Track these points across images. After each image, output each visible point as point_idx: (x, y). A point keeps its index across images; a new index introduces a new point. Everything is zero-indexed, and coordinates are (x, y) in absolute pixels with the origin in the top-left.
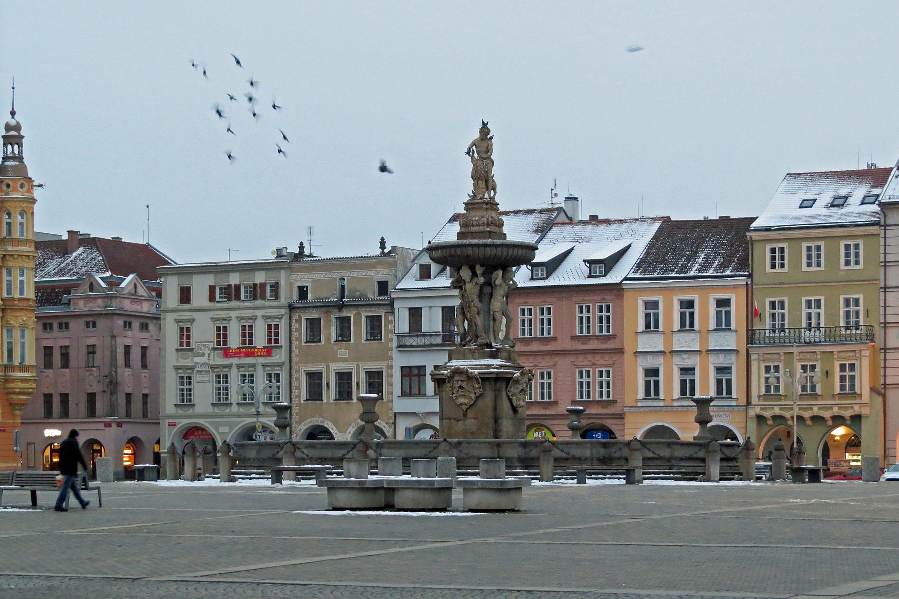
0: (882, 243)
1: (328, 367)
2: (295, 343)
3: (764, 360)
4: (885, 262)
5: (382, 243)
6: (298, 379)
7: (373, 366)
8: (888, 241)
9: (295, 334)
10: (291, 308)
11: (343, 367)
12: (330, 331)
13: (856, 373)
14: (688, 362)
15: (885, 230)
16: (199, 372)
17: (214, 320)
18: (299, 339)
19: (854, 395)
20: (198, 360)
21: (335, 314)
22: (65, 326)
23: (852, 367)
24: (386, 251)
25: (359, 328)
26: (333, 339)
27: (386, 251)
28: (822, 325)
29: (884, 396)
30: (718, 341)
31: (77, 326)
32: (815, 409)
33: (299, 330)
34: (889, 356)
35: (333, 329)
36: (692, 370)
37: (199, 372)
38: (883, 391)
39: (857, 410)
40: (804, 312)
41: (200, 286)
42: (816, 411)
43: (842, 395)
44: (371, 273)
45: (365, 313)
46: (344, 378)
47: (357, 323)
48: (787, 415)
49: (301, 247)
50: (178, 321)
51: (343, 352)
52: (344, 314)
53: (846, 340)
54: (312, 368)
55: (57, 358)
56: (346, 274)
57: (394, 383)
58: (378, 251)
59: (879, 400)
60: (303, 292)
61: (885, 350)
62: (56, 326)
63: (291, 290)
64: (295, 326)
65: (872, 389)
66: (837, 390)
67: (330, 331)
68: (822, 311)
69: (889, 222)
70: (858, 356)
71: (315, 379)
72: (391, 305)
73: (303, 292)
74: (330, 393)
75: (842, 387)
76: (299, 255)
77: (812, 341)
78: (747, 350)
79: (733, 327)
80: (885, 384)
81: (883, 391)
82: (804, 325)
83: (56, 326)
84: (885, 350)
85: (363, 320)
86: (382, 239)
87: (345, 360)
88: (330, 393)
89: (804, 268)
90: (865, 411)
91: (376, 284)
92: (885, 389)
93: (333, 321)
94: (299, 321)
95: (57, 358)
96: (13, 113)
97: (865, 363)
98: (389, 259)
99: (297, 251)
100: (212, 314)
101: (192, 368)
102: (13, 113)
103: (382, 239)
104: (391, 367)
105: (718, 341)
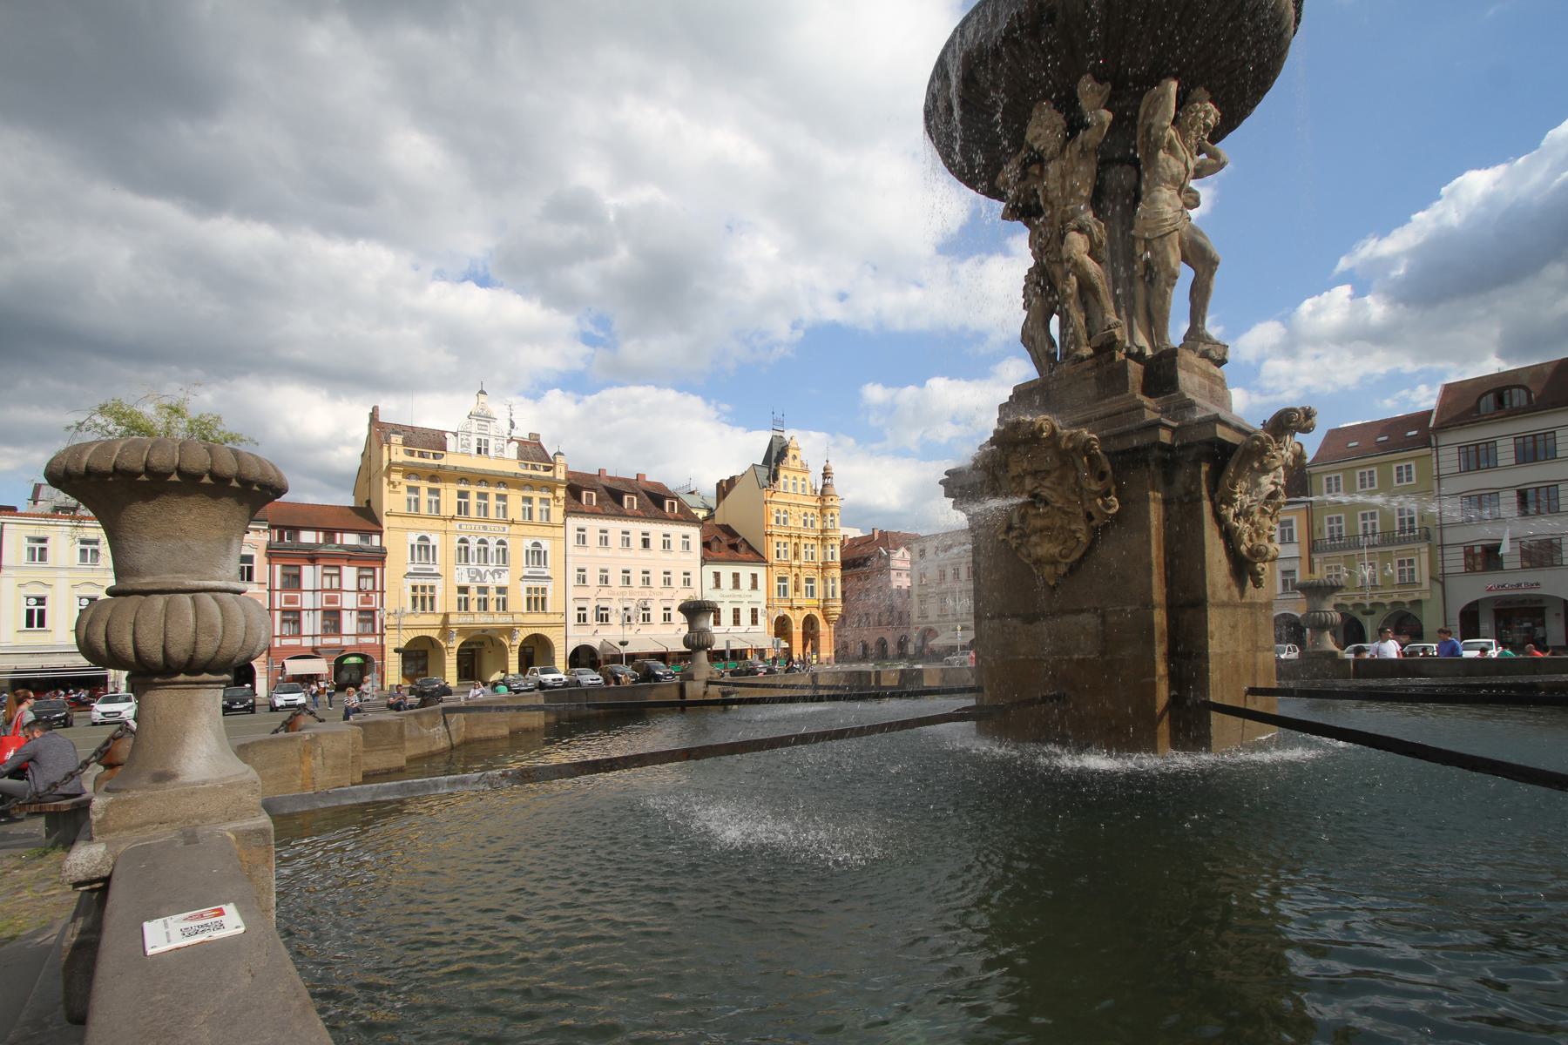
0: (1435, 460)
3: (1326, 562)
4: (1439, 475)
8: (1441, 459)
13: (1416, 567)
15: (1437, 450)
19: (1412, 584)
23: (1411, 562)
28: (1378, 530)
29: (1443, 584)
34: (1446, 551)
38: (1441, 579)
39: (1417, 596)
40: (1360, 523)
41: (930, 548)
48: (1349, 603)
53: (1401, 541)
59: (1438, 587)
61: (1442, 546)
66: (1397, 581)
68: (1377, 521)
69: (1440, 444)
78: (1310, 557)
79: (1296, 540)
80: (1443, 574)
81: (1441, 579)
82: (1361, 532)
84: (1442, 546)
97: (1425, 558)
101: (926, 595)
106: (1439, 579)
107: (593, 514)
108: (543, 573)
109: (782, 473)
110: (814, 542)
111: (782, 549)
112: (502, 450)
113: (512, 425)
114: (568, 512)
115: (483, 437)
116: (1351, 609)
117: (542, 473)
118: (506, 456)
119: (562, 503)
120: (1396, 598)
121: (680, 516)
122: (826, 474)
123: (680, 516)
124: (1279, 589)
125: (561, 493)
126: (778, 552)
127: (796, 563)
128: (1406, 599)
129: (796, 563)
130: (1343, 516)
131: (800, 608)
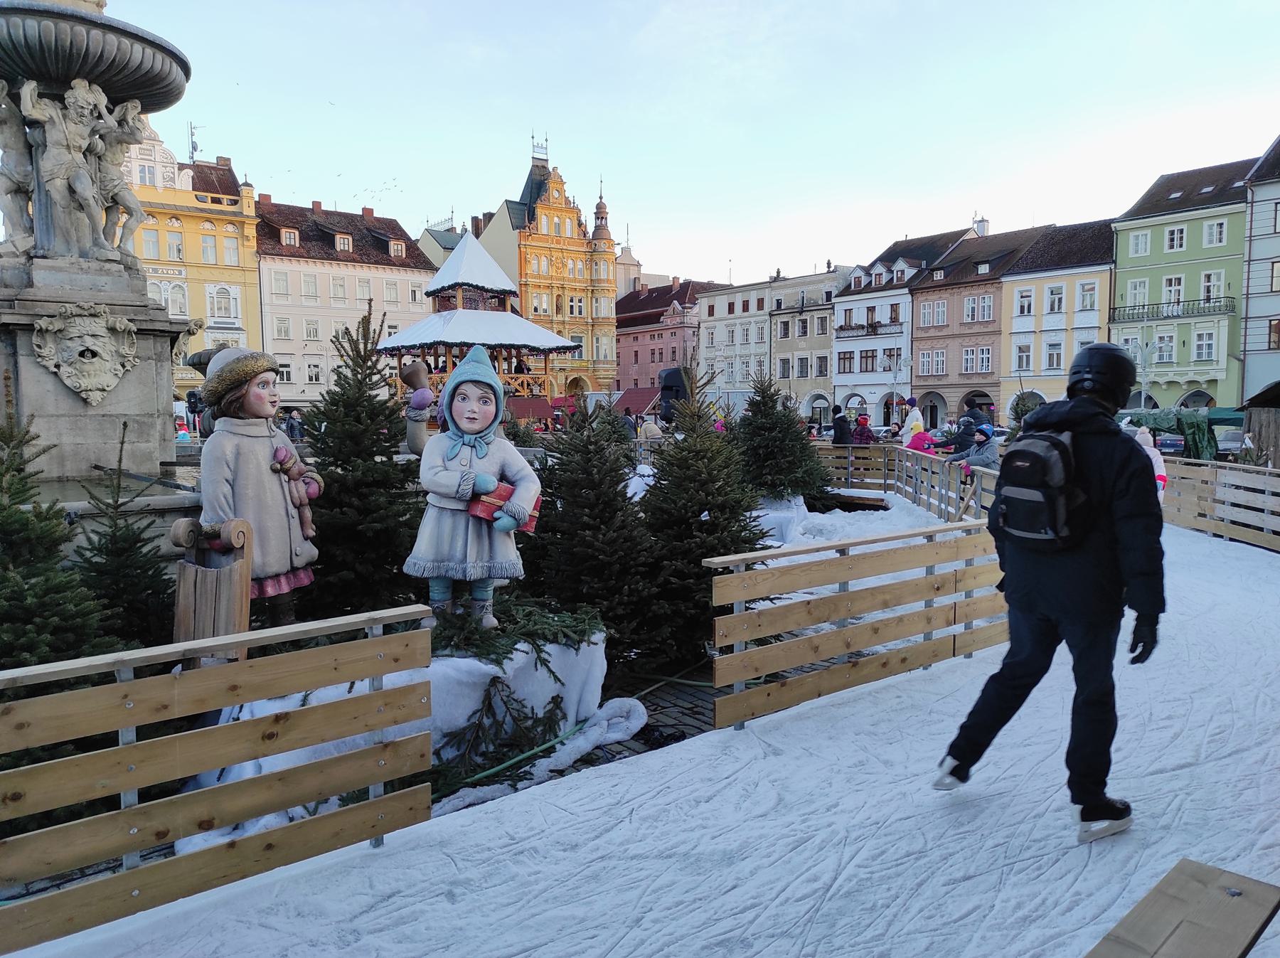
1: (793, 354)
2: (773, 339)
5: (829, 264)
6: (775, 364)
7: (821, 353)
9: (774, 333)
10: (771, 315)
11: (803, 354)
12: (795, 329)
13: (1214, 342)
14: (1054, 338)
16: (719, 361)
17: (727, 326)
18: (776, 336)
20: (717, 353)
21: (798, 317)
22: (661, 336)
23: (1210, 336)
24: (831, 269)
25: (814, 327)
26: (797, 335)
27: (831, 269)
29: (1243, 362)
30: (1082, 320)
31: (667, 334)
32: (1171, 374)
33: (776, 330)
35: (797, 328)
36: (1058, 345)
37: (719, 361)
42: (1171, 377)
43: (1199, 361)
44: (821, 286)
45: (817, 315)
46: (803, 361)
47: (812, 323)
49: (778, 272)
50: (707, 328)
51: (802, 344)
52: (804, 316)
54: (784, 356)
55: (657, 356)
56: (804, 289)
57: (833, 364)
58: (826, 270)
59: (1236, 364)
60: (779, 303)
61: (1247, 318)
62: (656, 336)
63: (772, 303)
64: (774, 327)
65: (1231, 355)
67: (795, 329)
70: (1216, 325)
71: (785, 362)
72: (833, 308)
73: (779, 303)
74: (795, 373)
75: (1199, 355)
76: (777, 278)
77: (1170, 314)
81: (1242, 357)
83: (656, 336)
84: (1247, 318)
85: (816, 320)
86: (829, 261)
87: (803, 349)
88: (795, 373)
89: (1166, 250)
90: (1221, 376)
91: (825, 295)
92: (1245, 354)
93: (797, 322)
94: (776, 324)
95: (657, 356)
96: (601, 198)
98: (833, 274)
99: (775, 275)
100: (725, 322)
102: (601, 198)
103: (829, 261)
104: (831, 353)
105: (1082, 320)
106: (1239, 357)
107: (292, 254)
108: (234, 324)
109: (541, 213)
110: (583, 295)
111: (576, 304)
112: (173, 180)
113: (195, 148)
114: (261, 252)
115: (147, 164)
116: (1204, 386)
117: (225, 207)
118: (178, 186)
119: (254, 243)
120: (1191, 377)
121: (408, 260)
122: (600, 213)
123: (408, 260)
124: (1045, 364)
125: (251, 231)
126: (572, 307)
127: (560, 318)
128: (1201, 379)
129: (560, 318)
130: (1183, 277)
131: (562, 370)
